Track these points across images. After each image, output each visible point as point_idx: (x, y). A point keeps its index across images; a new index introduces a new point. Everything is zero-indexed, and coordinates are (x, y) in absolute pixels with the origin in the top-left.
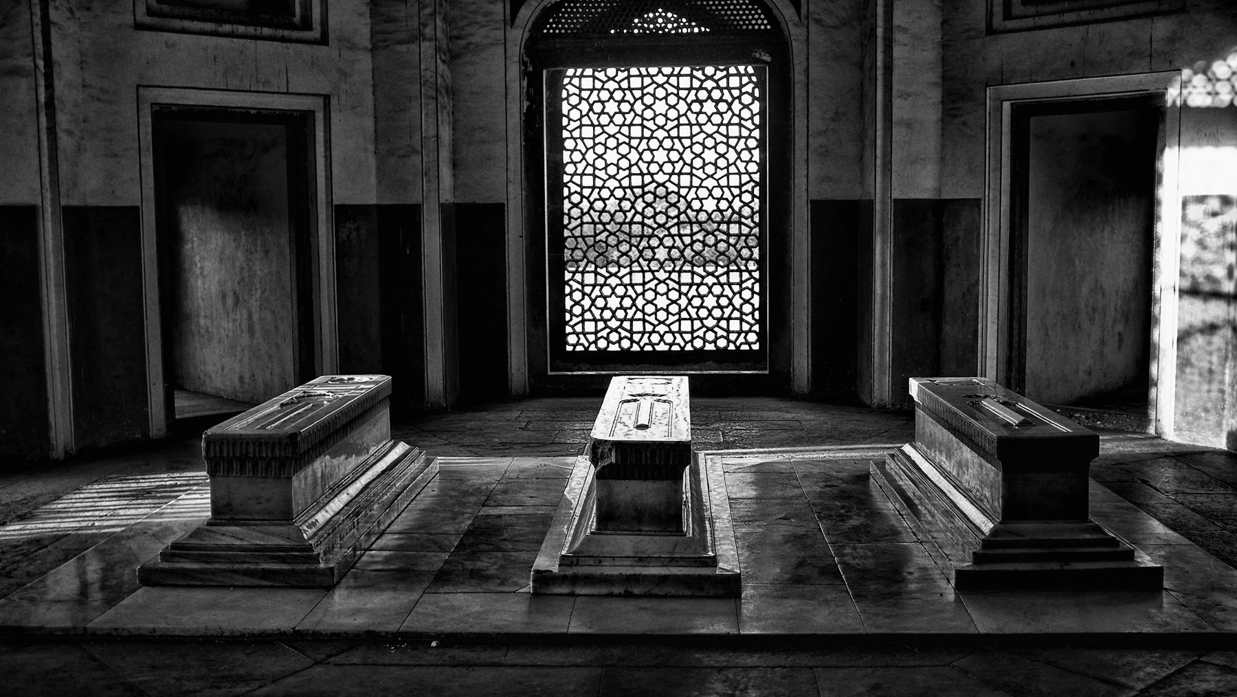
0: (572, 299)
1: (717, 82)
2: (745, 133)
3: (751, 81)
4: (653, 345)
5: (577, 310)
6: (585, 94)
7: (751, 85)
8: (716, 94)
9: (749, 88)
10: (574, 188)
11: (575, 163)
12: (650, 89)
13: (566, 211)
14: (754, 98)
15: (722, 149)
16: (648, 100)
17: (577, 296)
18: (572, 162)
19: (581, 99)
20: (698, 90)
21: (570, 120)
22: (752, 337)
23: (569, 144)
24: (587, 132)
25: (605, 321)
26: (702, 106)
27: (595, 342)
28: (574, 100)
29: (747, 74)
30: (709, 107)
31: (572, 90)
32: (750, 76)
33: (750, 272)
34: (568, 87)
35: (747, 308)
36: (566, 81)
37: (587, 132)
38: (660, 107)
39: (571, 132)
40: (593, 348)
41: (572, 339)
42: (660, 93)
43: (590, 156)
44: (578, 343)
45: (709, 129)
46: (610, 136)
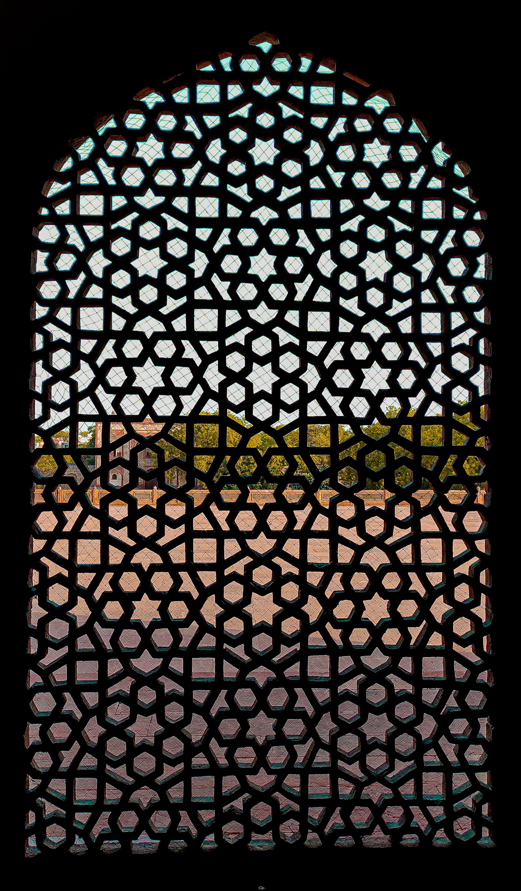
2: (459, 439)
7: (471, 332)
8: (392, 351)
9: (465, 338)
16: (236, 362)
20: (349, 339)
26: (359, 378)
29: (461, 305)
32: (468, 309)
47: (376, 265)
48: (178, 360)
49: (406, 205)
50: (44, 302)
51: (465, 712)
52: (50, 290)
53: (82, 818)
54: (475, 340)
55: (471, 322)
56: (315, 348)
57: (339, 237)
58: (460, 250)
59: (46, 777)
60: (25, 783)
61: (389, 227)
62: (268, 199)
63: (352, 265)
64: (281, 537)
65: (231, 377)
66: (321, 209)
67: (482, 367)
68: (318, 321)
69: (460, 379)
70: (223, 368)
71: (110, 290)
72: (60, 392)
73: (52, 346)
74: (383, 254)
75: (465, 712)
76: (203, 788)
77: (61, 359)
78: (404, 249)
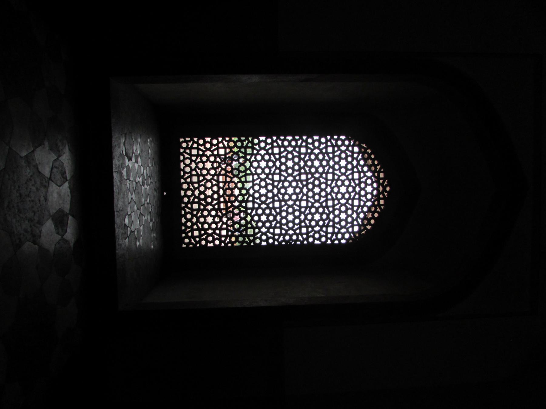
10: (245, 143)
11: (258, 144)
13: (233, 139)
15: (268, 225)
18: (260, 142)
21: (283, 141)
28: (293, 143)
37: (276, 150)
39: (276, 141)
49: (331, 223)
50: (307, 139)
52: (310, 141)
53: (188, 151)
55: (304, 239)
57: (323, 208)
58: (321, 236)
60: (196, 137)
61: (326, 219)
64: (253, 196)
65: (290, 183)
66: (330, 203)
71: (310, 154)
72: (286, 143)
73: (296, 141)
75: (214, 239)
76: (195, 179)
78: (321, 223)
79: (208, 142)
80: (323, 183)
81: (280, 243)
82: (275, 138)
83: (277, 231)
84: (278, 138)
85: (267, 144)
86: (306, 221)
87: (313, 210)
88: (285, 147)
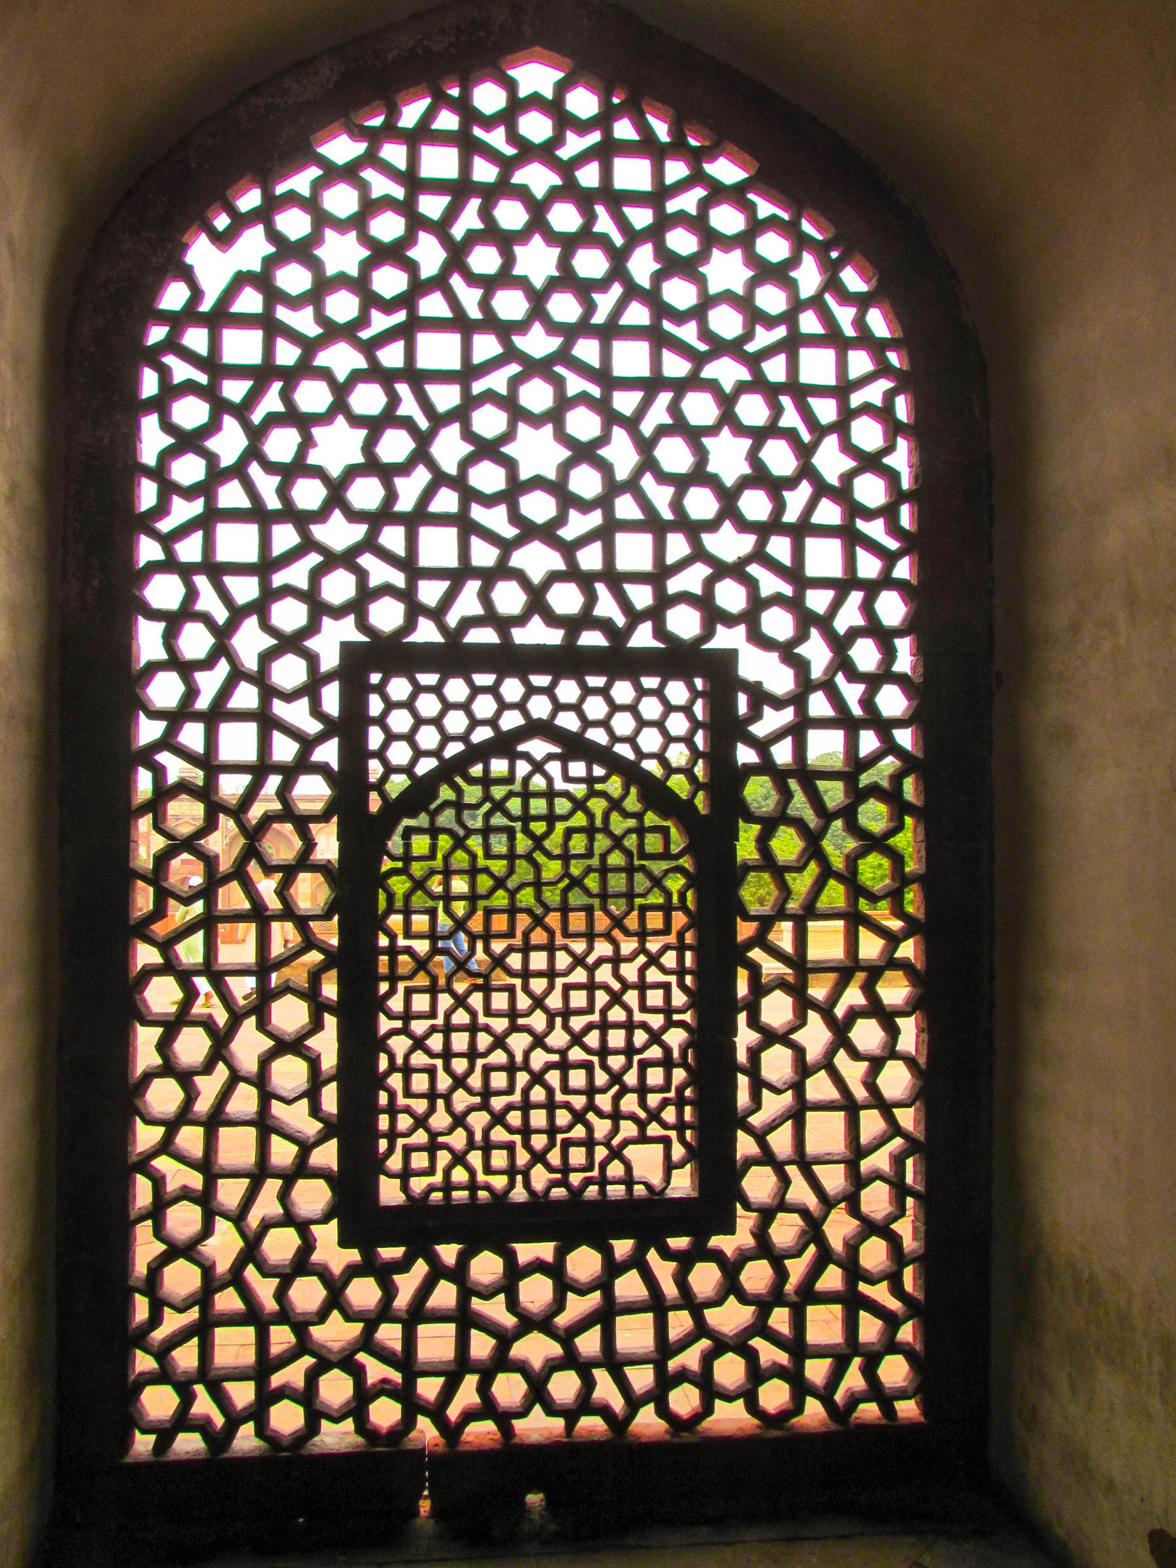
0: (159, 1232)
1: (754, 362)
3: (883, 370)
4: (504, 1419)
5: (182, 1278)
6: (235, 390)
7: (884, 384)
10: (175, 768)
11: (186, 669)
12: (497, 381)
14: (893, 429)
17: (184, 1219)
19: (220, 407)
22: (894, 1371)
23: (164, 592)
24: (237, 543)
25: (301, 1327)
27: (258, 1413)
28: (190, 413)
29: (865, 339)
30: (728, 457)
31: (182, 371)
32: (876, 347)
33: (886, 1108)
34: (170, 360)
35: (874, 1254)
36: (157, 334)
38: (537, 452)
40: (246, 1439)
41: (159, 1402)
42: (537, 396)
43: (250, 642)
44: (182, 1421)
45: (729, 544)
46: (333, 560)
47: (726, 271)
48: (389, 418)
51: (876, 1009)
54: (889, 396)
56: (625, 402)
59: (172, 1125)
61: (749, 209)
62: (545, 153)
63: (688, 268)
67: (902, 444)
68: (631, 358)
69: (870, 462)
70: (468, 435)
72: (188, 470)
74: (737, 254)
75: (876, 1009)
77: (190, 413)
79: (164, 1046)
80: (485, 213)
81: (910, 543)
82: (148, 550)
83: (823, 557)
84: (146, 523)
85: (186, 613)
86: (751, 348)
87: (679, 293)
88: (216, 475)
